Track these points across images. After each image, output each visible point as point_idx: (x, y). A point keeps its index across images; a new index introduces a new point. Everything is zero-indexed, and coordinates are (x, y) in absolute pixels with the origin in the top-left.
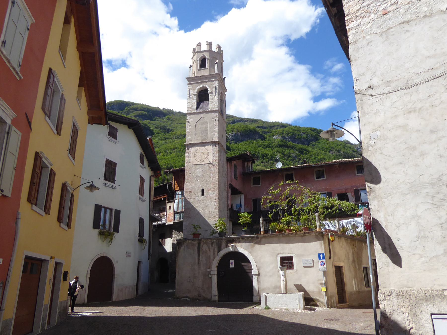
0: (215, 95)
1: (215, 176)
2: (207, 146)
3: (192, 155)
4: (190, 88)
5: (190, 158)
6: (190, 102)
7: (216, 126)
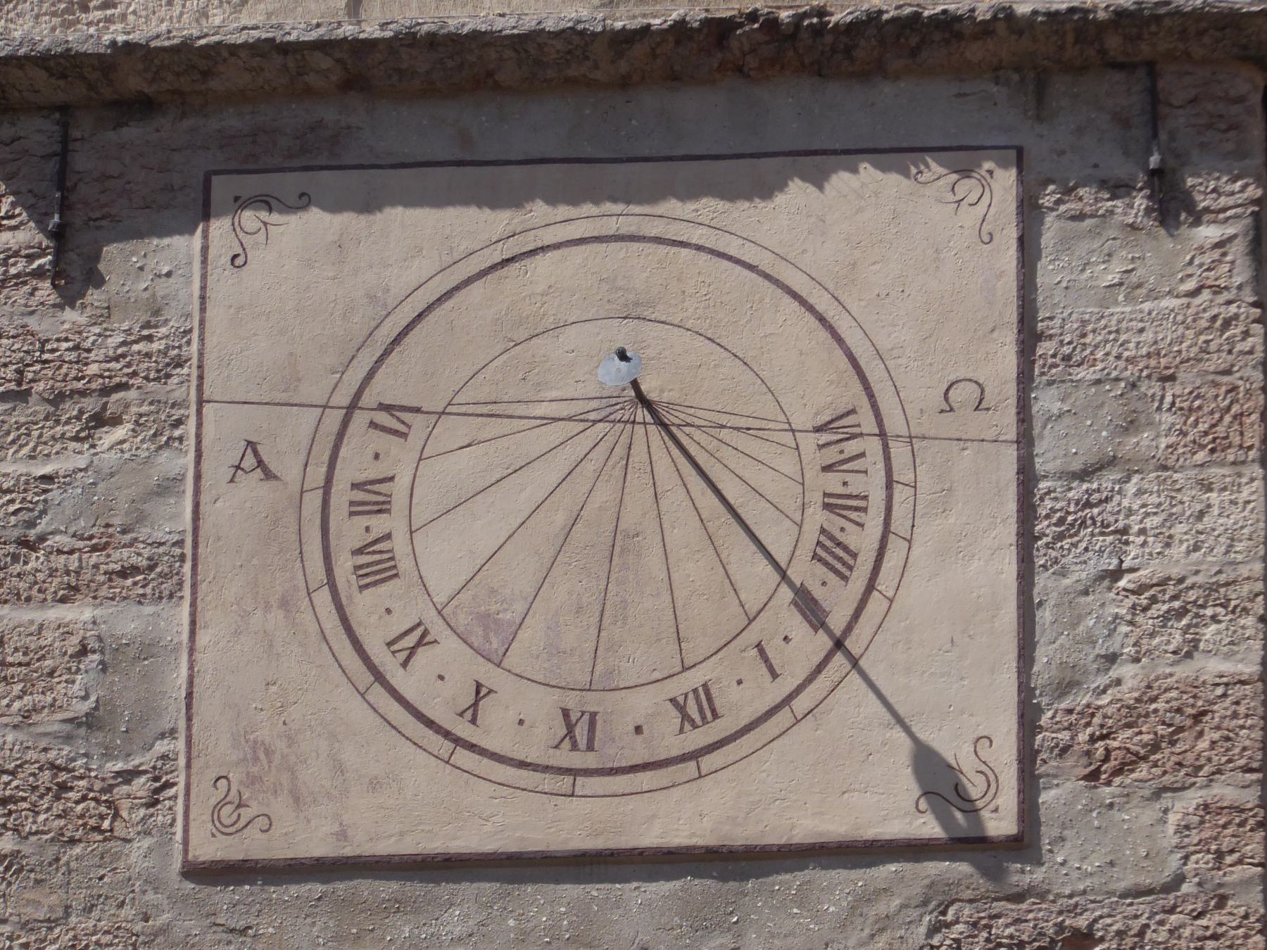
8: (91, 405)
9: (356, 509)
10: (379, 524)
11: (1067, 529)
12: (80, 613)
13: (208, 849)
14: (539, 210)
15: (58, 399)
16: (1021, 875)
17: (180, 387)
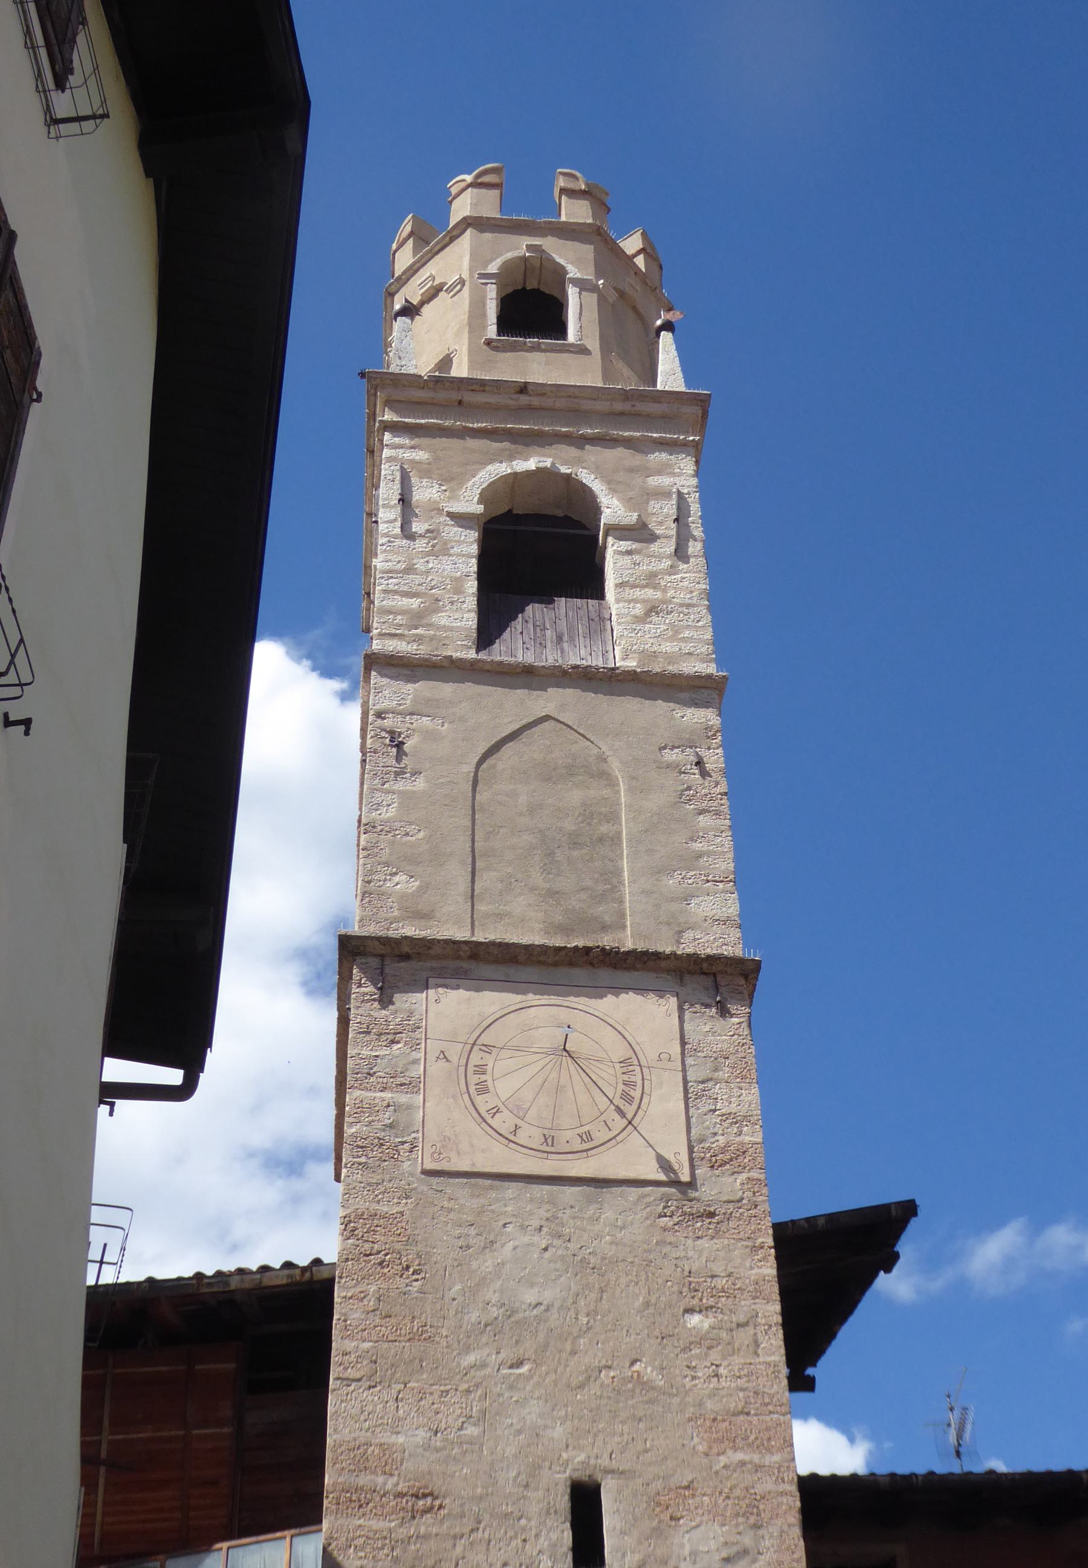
0: (681, 553)
1: (744, 1337)
2: (617, 989)
3: (437, 1069)
4: (412, 462)
5: (403, 1098)
6: (410, 570)
7: (704, 821)
8: (390, 1037)
9: (475, 1073)
10: (483, 1077)
11: (698, 1097)
12: (387, 1095)
13: (430, 1165)
14: (531, 996)
15: (380, 1035)
16: (693, 1194)
17: (419, 1034)
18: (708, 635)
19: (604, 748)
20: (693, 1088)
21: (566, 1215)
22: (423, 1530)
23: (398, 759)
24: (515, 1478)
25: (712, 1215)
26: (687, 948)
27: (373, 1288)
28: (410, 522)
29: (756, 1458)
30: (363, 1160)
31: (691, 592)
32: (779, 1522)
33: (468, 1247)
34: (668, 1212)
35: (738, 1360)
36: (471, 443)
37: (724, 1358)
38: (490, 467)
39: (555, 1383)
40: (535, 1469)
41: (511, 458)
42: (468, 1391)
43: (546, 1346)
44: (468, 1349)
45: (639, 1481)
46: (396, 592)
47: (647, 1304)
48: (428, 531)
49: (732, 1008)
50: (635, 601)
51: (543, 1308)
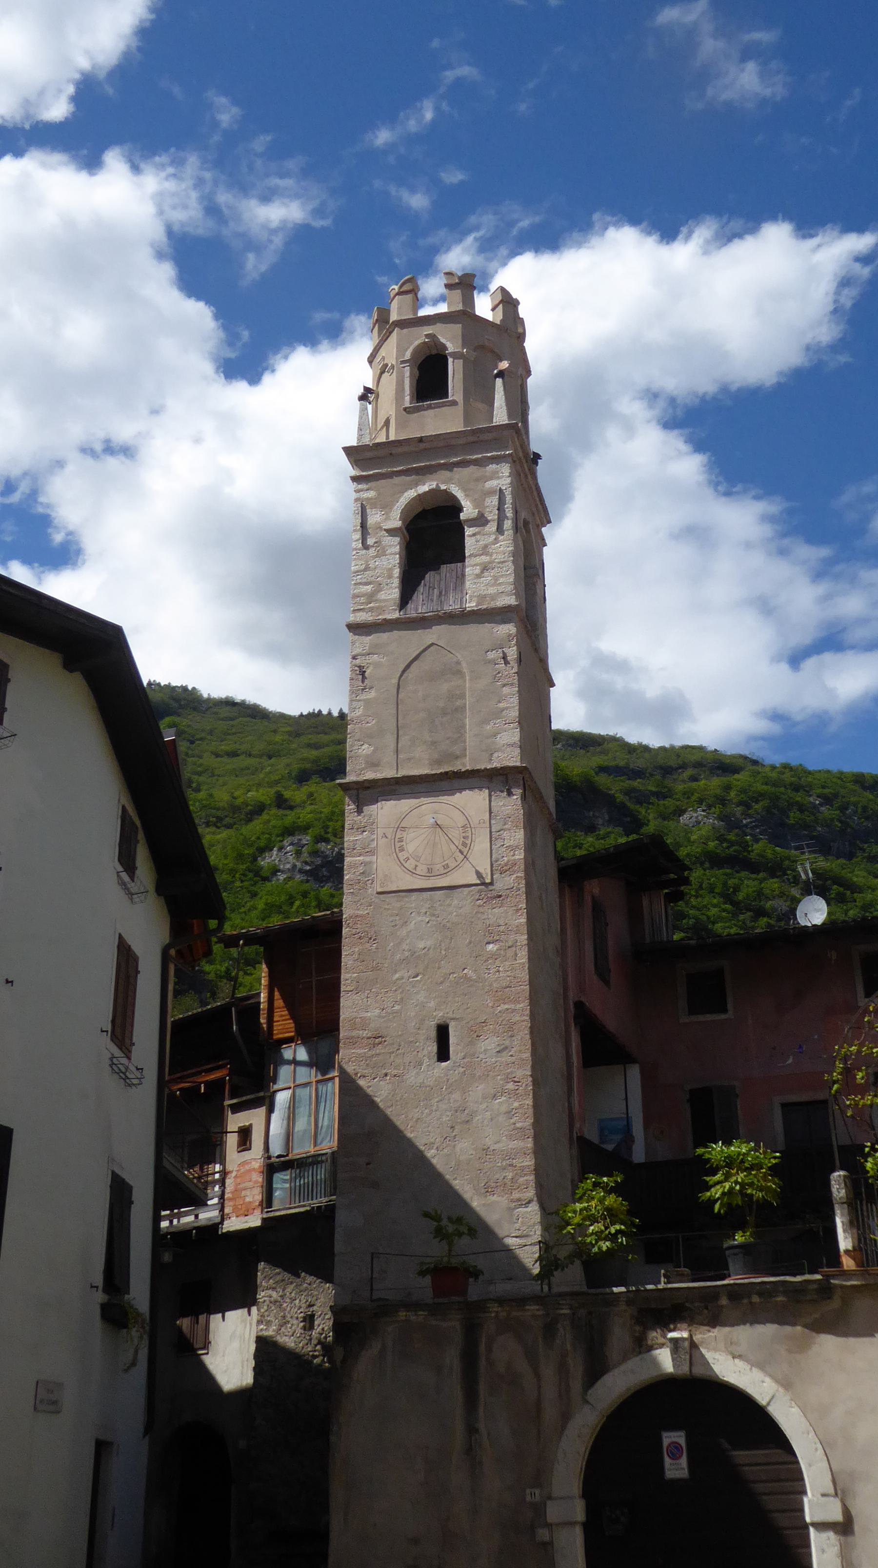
0: (500, 530)
1: (510, 952)
2: (460, 790)
3: (382, 842)
4: (368, 499)
5: (367, 859)
6: (367, 569)
7: (506, 690)
8: (362, 829)
9: (399, 842)
10: (402, 844)
11: (496, 839)
12: (361, 858)
13: (380, 890)
14: (422, 799)
15: (358, 829)
16: (491, 888)
17: (374, 826)
18: (511, 579)
19: (459, 657)
20: (495, 835)
21: (437, 905)
22: (378, 1051)
23: (363, 682)
24: (414, 1026)
25: (500, 896)
26: (496, 764)
27: (357, 949)
28: (366, 540)
29: (513, 1006)
30: (352, 891)
31: (504, 554)
32: (521, 1033)
33: (396, 925)
34: (481, 897)
35: (507, 963)
36: (397, 480)
37: (502, 962)
38: (406, 494)
39: (431, 982)
40: (422, 1021)
41: (416, 484)
42: (396, 990)
43: (427, 967)
44: (396, 972)
45: (464, 1022)
46: (360, 584)
47: (470, 942)
48: (376, 543)
49: (514, 791)
50: (476, 565)
51: (426, 949)
